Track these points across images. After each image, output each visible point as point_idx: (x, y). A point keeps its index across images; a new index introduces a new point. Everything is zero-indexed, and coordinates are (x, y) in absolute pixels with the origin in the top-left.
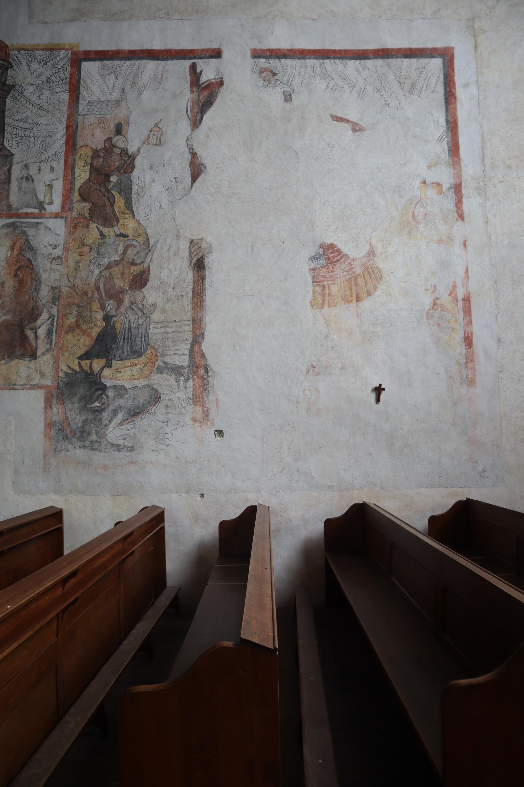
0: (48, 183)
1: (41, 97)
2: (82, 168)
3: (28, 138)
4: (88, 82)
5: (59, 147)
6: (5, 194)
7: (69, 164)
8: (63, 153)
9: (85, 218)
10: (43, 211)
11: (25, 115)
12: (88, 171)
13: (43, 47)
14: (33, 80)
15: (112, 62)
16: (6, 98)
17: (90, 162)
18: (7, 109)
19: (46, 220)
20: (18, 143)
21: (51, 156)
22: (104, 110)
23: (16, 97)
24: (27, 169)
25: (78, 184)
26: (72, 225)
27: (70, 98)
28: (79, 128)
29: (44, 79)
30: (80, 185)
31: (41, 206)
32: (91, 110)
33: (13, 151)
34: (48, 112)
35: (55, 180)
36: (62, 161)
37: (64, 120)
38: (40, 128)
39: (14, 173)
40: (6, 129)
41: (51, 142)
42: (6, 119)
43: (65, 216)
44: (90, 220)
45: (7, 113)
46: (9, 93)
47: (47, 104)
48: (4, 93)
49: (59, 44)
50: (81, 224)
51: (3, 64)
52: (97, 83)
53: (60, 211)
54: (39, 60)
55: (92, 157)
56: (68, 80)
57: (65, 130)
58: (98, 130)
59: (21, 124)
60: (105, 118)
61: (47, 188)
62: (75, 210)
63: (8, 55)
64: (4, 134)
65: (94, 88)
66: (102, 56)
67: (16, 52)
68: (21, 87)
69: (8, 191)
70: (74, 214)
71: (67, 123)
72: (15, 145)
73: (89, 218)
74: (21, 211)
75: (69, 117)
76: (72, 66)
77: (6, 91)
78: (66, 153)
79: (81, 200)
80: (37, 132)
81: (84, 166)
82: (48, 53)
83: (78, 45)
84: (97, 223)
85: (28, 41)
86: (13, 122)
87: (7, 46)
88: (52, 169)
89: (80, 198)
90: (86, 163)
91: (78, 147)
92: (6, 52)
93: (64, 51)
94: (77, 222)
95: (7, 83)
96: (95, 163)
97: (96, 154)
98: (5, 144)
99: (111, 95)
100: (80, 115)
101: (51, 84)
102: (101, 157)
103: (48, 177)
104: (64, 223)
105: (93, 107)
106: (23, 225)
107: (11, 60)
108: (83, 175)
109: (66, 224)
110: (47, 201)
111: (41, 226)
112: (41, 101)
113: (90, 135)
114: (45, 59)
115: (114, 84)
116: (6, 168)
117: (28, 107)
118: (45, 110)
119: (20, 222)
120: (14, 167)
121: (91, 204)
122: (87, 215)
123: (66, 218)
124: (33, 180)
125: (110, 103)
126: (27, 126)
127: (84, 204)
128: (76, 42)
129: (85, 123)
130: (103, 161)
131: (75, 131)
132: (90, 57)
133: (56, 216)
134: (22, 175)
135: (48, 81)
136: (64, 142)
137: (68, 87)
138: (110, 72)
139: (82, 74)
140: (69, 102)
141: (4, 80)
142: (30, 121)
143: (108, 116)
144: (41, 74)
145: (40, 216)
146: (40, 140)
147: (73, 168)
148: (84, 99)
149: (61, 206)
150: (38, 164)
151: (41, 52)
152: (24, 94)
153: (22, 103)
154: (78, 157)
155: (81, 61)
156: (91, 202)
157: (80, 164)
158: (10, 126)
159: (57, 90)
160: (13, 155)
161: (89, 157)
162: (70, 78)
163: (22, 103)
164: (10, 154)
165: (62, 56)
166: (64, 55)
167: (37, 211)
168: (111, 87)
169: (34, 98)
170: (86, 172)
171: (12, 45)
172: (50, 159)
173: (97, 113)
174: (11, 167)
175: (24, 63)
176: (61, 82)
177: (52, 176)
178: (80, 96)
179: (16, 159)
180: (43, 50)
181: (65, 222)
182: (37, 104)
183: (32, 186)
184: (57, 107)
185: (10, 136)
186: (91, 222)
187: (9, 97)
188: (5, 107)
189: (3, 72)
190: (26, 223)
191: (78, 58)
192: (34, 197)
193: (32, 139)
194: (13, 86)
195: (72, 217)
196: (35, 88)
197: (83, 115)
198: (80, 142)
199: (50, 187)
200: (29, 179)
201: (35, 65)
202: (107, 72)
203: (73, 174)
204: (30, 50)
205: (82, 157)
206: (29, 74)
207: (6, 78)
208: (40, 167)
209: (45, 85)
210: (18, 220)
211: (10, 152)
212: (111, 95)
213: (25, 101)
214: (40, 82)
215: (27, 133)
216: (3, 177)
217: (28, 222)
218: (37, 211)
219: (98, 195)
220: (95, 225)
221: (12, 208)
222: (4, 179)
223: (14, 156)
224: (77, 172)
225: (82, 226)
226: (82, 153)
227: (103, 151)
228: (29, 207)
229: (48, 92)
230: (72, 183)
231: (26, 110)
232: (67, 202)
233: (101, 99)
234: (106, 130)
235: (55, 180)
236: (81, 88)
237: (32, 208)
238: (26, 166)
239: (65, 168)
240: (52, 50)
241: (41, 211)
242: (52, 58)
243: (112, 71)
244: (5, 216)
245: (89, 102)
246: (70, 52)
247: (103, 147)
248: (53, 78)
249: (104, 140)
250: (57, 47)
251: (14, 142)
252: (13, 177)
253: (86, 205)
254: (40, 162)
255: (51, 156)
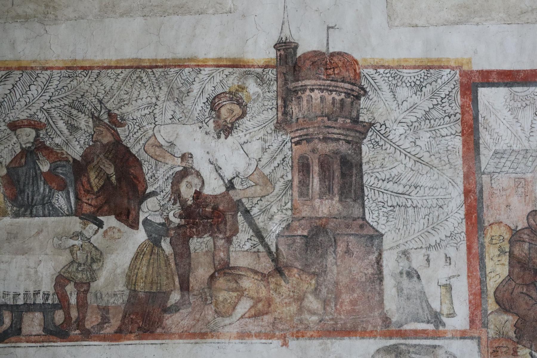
0: (443, 282)
1: (417, 143)
2: (496, 259)
3: (403, 208)
4: (492, 120)
5: (456, 225)
6: (377, 298)
7: (474, 251)
8: (463, 234)
9: (509, 339)
10: (441, 328)
11: (394, 172)
12: (507, 263)
13: (413, 63)
14: (402, 116)
15: (525, 88)
16: (361, 143)
17: (507, 250)
18: (364, 161)
19: (447, 341)
20: (387, 215)
21: (444, 238)
22: (522, 165)
23: (377, 142)
24: (408, 259)
25: (492, 284)
26: (490, 350)
27: (464, 146)
28: (485, 195)
29: (420, 113)
30: (496, 286)
31: (436, 318)
32: (500, 165)
33: (381, 229)
34: (432, 167)
35: (454, 277)
36: (463, 247)
37: (460, 180)
38: (421, 192)
39: (387, 265)
40: (366, 193)
41: (442, 217)
42: (365, 178)
43: (476, 335)
44: (518, 343)
45: (365, 167)
46: (364, 134)
47: (427, 154)
48: (358, 134)
49: (439, 60)
50: (504, 350)
51: (352, 90)
52: (504, 122)
53: (468, 328)
54: (408, 84)
55: (510, 242)
56: (459, 116)
57: (463, 197)
58: (516, 198)
59: (390, 186)
60: (524, 179)
61: (443, 290)
62: (492, 327)
63: (357, 75)
64: (363, 201)
65: (502, 130)
66: (509, 78)
67: (372, 71)
68: (384, 127)
69: (381, 293)
70: (492, 333)
71: (464, 186)
72: (383, 220)
73: (515, 340)
74: (407, 327)
75: (466, 177)
76: (463, 95)
77: (360, 132)
78: (468, 233)
79: (499, 310)
80: (416, 199)
81: (499, 255)
82: (423, 72)
83: (469, 62)
84: (530, 348)
85: (390, 54)
86: (376, 182)
87: (356, 61)
88: (448, 259)
89: (498, 307)
90: (502, 251)
91: (486, 224)
92: (355, 70)
93: (448, 71)
94: (496, 345)
95: (361, 119)
96: (517, 251)
97: (516, 237)
98: (367, 217)
99: (529, 141)
100: (484, 173)
101: (432, 121)
102: (524, 241)
103: (443, 273)
104: (477, 347)
105: (503, 161)
106: (411, 350)
107: (364, 83)
108: (499, 269)
109: (479, 348)
110: (445, 311)
111: (440, 352)
112: (418, 149)
113: (503, 207)
114: (418, 83)
115: (532, 123)
116: (373, 257)
117: (399, 159)
118: (427, 164)
119: (406, 345)
120: (386, 255)
121: (516, 318)
122: (512, 334)
123: (479, 338)
124: (419, 277)
125: (529, 155)
126: (401, 189)
127: (505, 317)
128: (466, 57)
129: (494, 185)
130: (529, 249)
131: (480, 199)
132: (491, 80)
133: (463, 336)
134: (401, 268)
135: (427, 116)
136: (463, 217)
137: (459, 128)
138: (524, 105)
139: (481, 107)
140: (464, 152)
141: (354, 114)
142: (404, 182)
143: (529, 176)
144: (413, 108)
145: (436, 335)
146: (424, 211)
147: (482, 259)
148: (487, 148)
149: (468, 320)
150: (424, 251)
151: (411, 71)
152: (390, 137)
153: (388, 151)
154: (487, 240)
155: (477, 87)
156: (517, 314)
157: (492, 252)
158: (372, 188)
159: (444, 132)
160: (382, 235)
161: (506, 242)
162: (463, 114)
163: (388, 151)
164: (376, 233)
165: (445, 78)
166: (449, 76)
167: (430, 327)
168: (527, 127)
169: (406, 144)
170: (503, 264)
171: (365, 60)
172: (443, 244)
173: (511, 170)
174: (380, 255)
175: (385, 87)
176: (447, 119)
177: (448, 271)
178: (481, 141)
179: (387, 242)
180: (415, 67)
181: (479, 345)
182: (413, 153)
183: (418, 287)
184: (446, 159)
185: (374, 205)
186: (519, 346)
187: (365, 141)
188: (361, 159)
189: (352, 103)
190: (415, 346)
191: (472, 83)
192: (424, 304)
193: (410, 210)
194: (371, 125)
195: (488, 338)
196: (407, 128)
197: (489, 173)
198: (489, 217)
199: (448, 288)
200: (412, 274)
201: (403, 92)
202: (519, 106)
203: (483, 267)
204: (394, 69)
205: (494, 242)
206: (394, 106)
207: (358, 111)
208: (428, 256)
209: (423, 123)
210: (403, 341)
211: (377, 231)
212: (529, 141)
213: (392, 149)
214: (414, 119)
215: (402, 200)
216: (370, 271)
217: (419, 345)
218: (430, 327)
219: (527, 303)
220: (528, 351)
221: (390, 323)
222: (372, 274)
223: (384, 237)
224: (489, 265)
225: (506, 353)
226: (493, 234)
227: (526, 231)
228: (417, 320)
229: (428, 135)
230: (482, 283)
231: (396, 164)
232: (478, 312)
233: (514, 147)
234: (527, 198)
235: (454, 277)
236: (481, 129)
237: (423, 322)
238: (405, 253)
239: (468, 259)
240: (429, 68)
241: (437, 326)
242: (430, 80)
243: (528, 103)
244: (381, 335)
245: (496, 153)
246: (458, 72)
247: (526, 225)
248: (435, 113)
249: (526, 213)
250: (436, 64)
251: (381, 214)
252: (386, 271)
253: (510, 319)
254: (429, 247)
255: (444, 238)
